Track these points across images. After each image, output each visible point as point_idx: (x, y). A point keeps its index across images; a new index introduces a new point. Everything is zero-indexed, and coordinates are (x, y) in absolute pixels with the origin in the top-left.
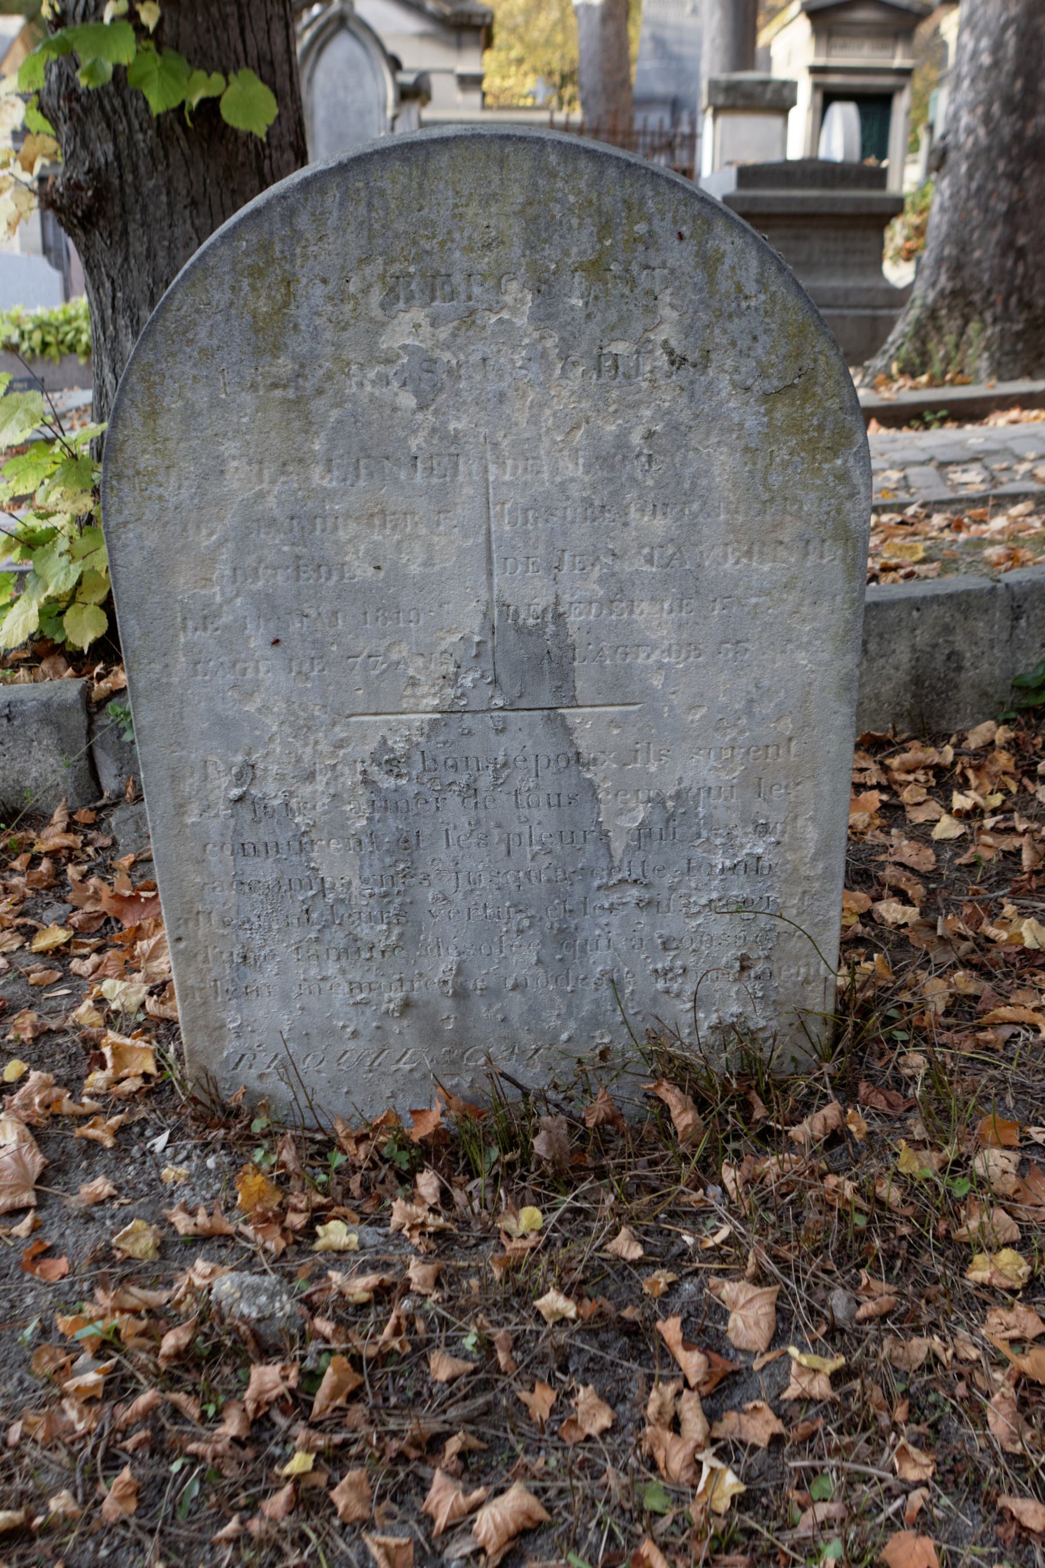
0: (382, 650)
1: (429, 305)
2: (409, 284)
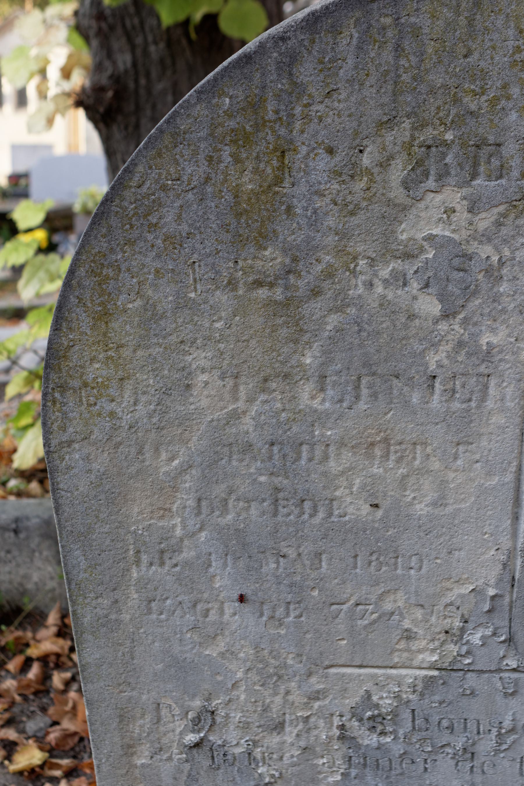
0: (373, 598)
1: (468, 183)
2: (444, 155)
